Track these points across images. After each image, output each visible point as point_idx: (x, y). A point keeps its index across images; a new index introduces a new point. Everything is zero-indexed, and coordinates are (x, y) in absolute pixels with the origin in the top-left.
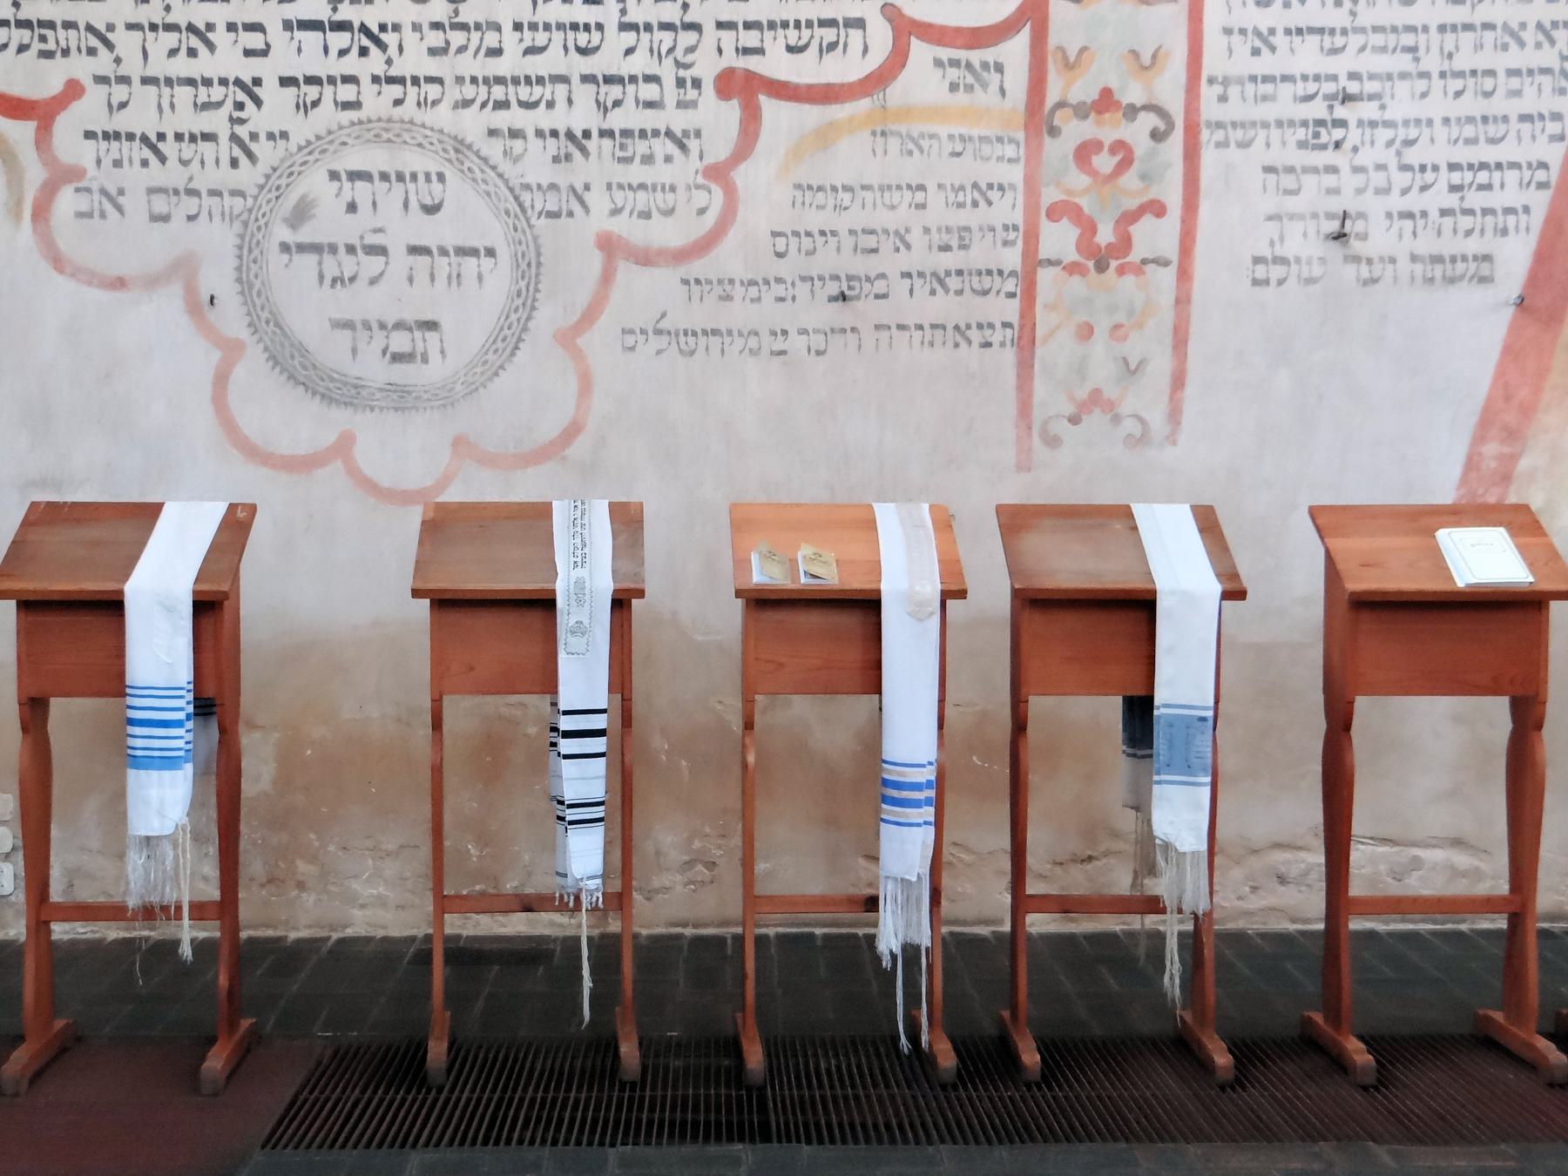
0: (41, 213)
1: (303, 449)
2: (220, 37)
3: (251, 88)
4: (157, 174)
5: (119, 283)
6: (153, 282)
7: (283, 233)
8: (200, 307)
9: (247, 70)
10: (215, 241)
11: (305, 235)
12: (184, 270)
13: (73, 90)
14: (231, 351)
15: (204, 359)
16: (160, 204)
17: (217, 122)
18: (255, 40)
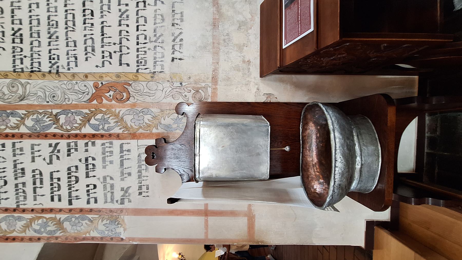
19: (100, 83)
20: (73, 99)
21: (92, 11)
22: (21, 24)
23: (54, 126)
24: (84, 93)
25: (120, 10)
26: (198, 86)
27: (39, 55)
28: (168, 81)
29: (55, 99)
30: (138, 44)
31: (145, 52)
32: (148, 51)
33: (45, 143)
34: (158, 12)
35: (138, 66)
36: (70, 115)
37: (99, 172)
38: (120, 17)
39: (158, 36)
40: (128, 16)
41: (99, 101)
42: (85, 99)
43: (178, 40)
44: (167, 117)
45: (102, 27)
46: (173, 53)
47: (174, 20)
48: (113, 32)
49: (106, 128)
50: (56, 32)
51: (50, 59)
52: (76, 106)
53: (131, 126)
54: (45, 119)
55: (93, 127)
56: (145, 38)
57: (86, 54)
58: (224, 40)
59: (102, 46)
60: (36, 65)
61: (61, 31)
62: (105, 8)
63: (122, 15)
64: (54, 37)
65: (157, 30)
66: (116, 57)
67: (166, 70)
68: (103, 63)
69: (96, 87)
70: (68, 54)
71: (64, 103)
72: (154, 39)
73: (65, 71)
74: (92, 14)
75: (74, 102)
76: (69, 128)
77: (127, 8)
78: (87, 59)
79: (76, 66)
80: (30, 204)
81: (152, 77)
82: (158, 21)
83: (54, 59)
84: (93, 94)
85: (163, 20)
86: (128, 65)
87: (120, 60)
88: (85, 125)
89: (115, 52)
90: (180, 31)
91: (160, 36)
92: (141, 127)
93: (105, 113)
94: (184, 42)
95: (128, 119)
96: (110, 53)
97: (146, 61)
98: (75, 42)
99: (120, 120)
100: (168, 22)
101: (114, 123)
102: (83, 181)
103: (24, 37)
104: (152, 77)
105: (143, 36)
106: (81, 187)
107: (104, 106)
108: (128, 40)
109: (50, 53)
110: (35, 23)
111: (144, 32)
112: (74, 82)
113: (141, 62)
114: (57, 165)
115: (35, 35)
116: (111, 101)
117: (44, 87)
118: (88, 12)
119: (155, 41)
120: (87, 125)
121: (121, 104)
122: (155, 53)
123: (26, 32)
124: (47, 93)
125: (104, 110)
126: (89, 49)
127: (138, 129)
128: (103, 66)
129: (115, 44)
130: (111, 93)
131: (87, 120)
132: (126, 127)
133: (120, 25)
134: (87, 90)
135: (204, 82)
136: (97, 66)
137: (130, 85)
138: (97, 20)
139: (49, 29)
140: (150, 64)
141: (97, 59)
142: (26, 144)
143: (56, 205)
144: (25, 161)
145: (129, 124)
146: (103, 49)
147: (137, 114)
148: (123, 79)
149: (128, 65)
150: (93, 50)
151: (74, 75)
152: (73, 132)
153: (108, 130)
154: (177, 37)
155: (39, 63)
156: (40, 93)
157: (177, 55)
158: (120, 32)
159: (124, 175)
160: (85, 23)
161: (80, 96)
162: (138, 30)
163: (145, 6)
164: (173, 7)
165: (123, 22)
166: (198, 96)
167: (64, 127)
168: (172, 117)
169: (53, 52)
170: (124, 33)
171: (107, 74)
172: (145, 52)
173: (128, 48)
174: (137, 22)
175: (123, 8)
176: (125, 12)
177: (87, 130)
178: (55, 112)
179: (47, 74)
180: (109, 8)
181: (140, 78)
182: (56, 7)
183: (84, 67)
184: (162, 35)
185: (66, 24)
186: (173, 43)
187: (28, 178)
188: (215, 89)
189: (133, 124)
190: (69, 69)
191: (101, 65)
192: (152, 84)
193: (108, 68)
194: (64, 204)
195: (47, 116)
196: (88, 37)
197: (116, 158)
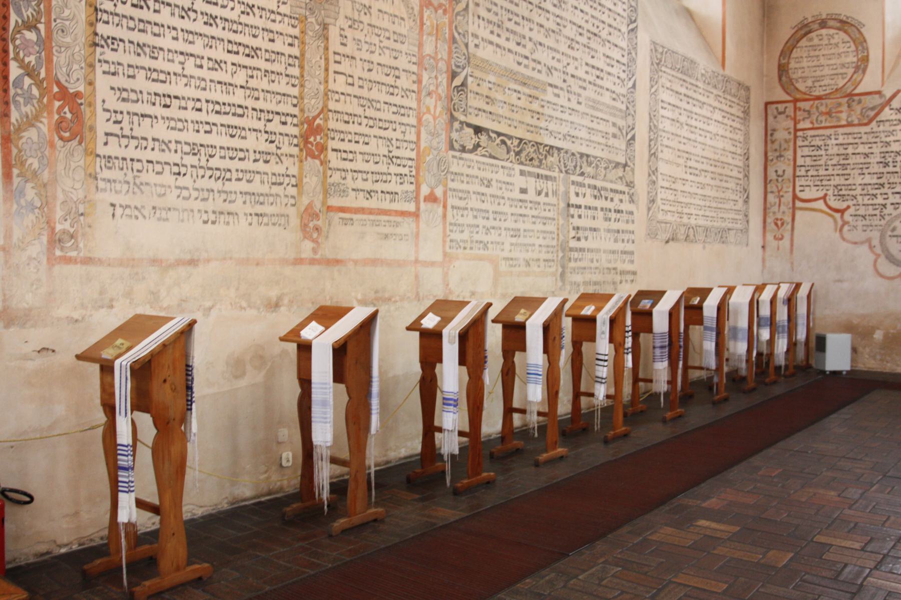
0: (841, 230)
1: (892, 275)
2: (879, 196)
3: (884, 206)
4: (864, 222)
5: (855, 243)
6: (862, 243)
7: (889, 233)
8: (871, 248)
9: (884, 202)
10: (875, 235)
11: (895, 233)
12: (869, 241)
13: (848, 207)
14: (878, 256)
15: (872, 257)
16: (865, 228)
17: (877, 212)
18: (886, 196)
19: (82, 101)
20: (60, 59)
21: (169, 107)
22: (155, 11)
23: (20, 21)
24: (68, 75)
25: (170, 142)
26: (79, 239)
27: (118, 25)
28: (85, 197)
29: (60, 32)
30: (132, 160)
31: (122, 169)
32: (122, 173)
34: (168, 190)
35: (104, 157)
36: (37, 48)
38: (163, 141)
39: (142, 187)
40: (163, 151)
41: (57, 96)
42: (60, 76)
43: (137, 213)
44: (34, 191)
45: (150, 117)
46: (121, 206)
47: (160, 209)
48: (144, 129)
49: (18, 98)
50: (145, 54)
51: (113, 38)
52: (49, 60)
53: (22, 137)
54: (30, 10)
55: (19, 79)
56: (138, 171)
57: (119, 89)
58: (137, 274)
59: (128, 113)
60: (105, 17)
61: (145, 61)
62: (173, 124)
63: (165, 143)
64: (139, 51)
65: (148, 187)
66: (115, 129)
67: (100, 196)
68: (108, 111)
69: (78, 94)
70: (119, 64)
71: (54, 44)
72: (138, 182)
73: (98, 56)
74: (166, 106)
75: (55, 59)
76: (18, 42)
77: (173, 151)
78: (112, 88)
79: (104, 72)
81: (90, 175)
82: (158, 189)
83: (113, 43)
84: (67, 88)
85: (160, 196)
86: (106, 144)
87: (111, 134)
88: (21, 67)
89: (122, 129)
90: (147, 216)
91: (141, 190)
92: (20, 151)
93: (40, 101)
94: (134, 220)
95: (31, 134)
96: (120, 122)
97: (110, 168)
98: (133, 77)
99: (30, 122)
100: (159, 202)
101: (26, 113)
103: (138, 10)
104: (90, 175)
105: (140, 168)
107: (50, 102)
108: (136, 147)
109: (121, 40)
110: (156, 29)
111: (145, 170)
112: (83, 65)
113: (109, 162)
115: (141, 26)
116: (59, 112)
117: (74, 21)
118: (168, 101)
119: (135, 184)
120: (21, 71)
121: (53, 127)
122: (120, 182)
124: (67, 23)
125: (45, 100)
126: (125, 95)
127: (17, 147)
128: (105, 110)
129: (132, 129)
130: (69, 116)
131: (30, 72)
132: (19, 130)
133: (154, 140)
134: (72, 81)
135: (85, 246)
136: (104, 101)
137: (80, 143)
138: (158, 111)
139: (149, 46)
140: (107, 174)
141: (113, 103)
145: (25, 134)
146: (125, 113)
147: (40, 149)
148: (88, 135)
149: (106, 144)
150: (124, 100)
151: (92, 66)
152: (11, 48)
153: (15, 102)
154: (140, 212)
155: (107, 23)
156: (67, 13)
157: (119, 211)
158: (146, 139)
160: (156, 94)
161: (64, 70)
162: (148, 162)
163: (175, 174)
164: (174, 209)
165: (157, 143)
166: (66, 237)
167: (18, 36)
168: (36, 199)
169: (121, 44)
170: (144, 143)
171: (94, 113)
172: (122, 169)
173: (126, 146)
174: (158, 162)
175: (173, 146)
176: (168, 148)
178: (41, 27)
179: (93, 28)
180: (172, 128)
181: (90, 158)
182: (173, 61)
183: (103, 83)
184: (142, 192)
185: (155, 70)
186: (133, 207)
188: (76, 262)
189: (24, 140)
190: (100, 61)
191: (106, 106)
192: (80, 175)
193: (101, 116)
195: (34, 13)
196: (140, 96)
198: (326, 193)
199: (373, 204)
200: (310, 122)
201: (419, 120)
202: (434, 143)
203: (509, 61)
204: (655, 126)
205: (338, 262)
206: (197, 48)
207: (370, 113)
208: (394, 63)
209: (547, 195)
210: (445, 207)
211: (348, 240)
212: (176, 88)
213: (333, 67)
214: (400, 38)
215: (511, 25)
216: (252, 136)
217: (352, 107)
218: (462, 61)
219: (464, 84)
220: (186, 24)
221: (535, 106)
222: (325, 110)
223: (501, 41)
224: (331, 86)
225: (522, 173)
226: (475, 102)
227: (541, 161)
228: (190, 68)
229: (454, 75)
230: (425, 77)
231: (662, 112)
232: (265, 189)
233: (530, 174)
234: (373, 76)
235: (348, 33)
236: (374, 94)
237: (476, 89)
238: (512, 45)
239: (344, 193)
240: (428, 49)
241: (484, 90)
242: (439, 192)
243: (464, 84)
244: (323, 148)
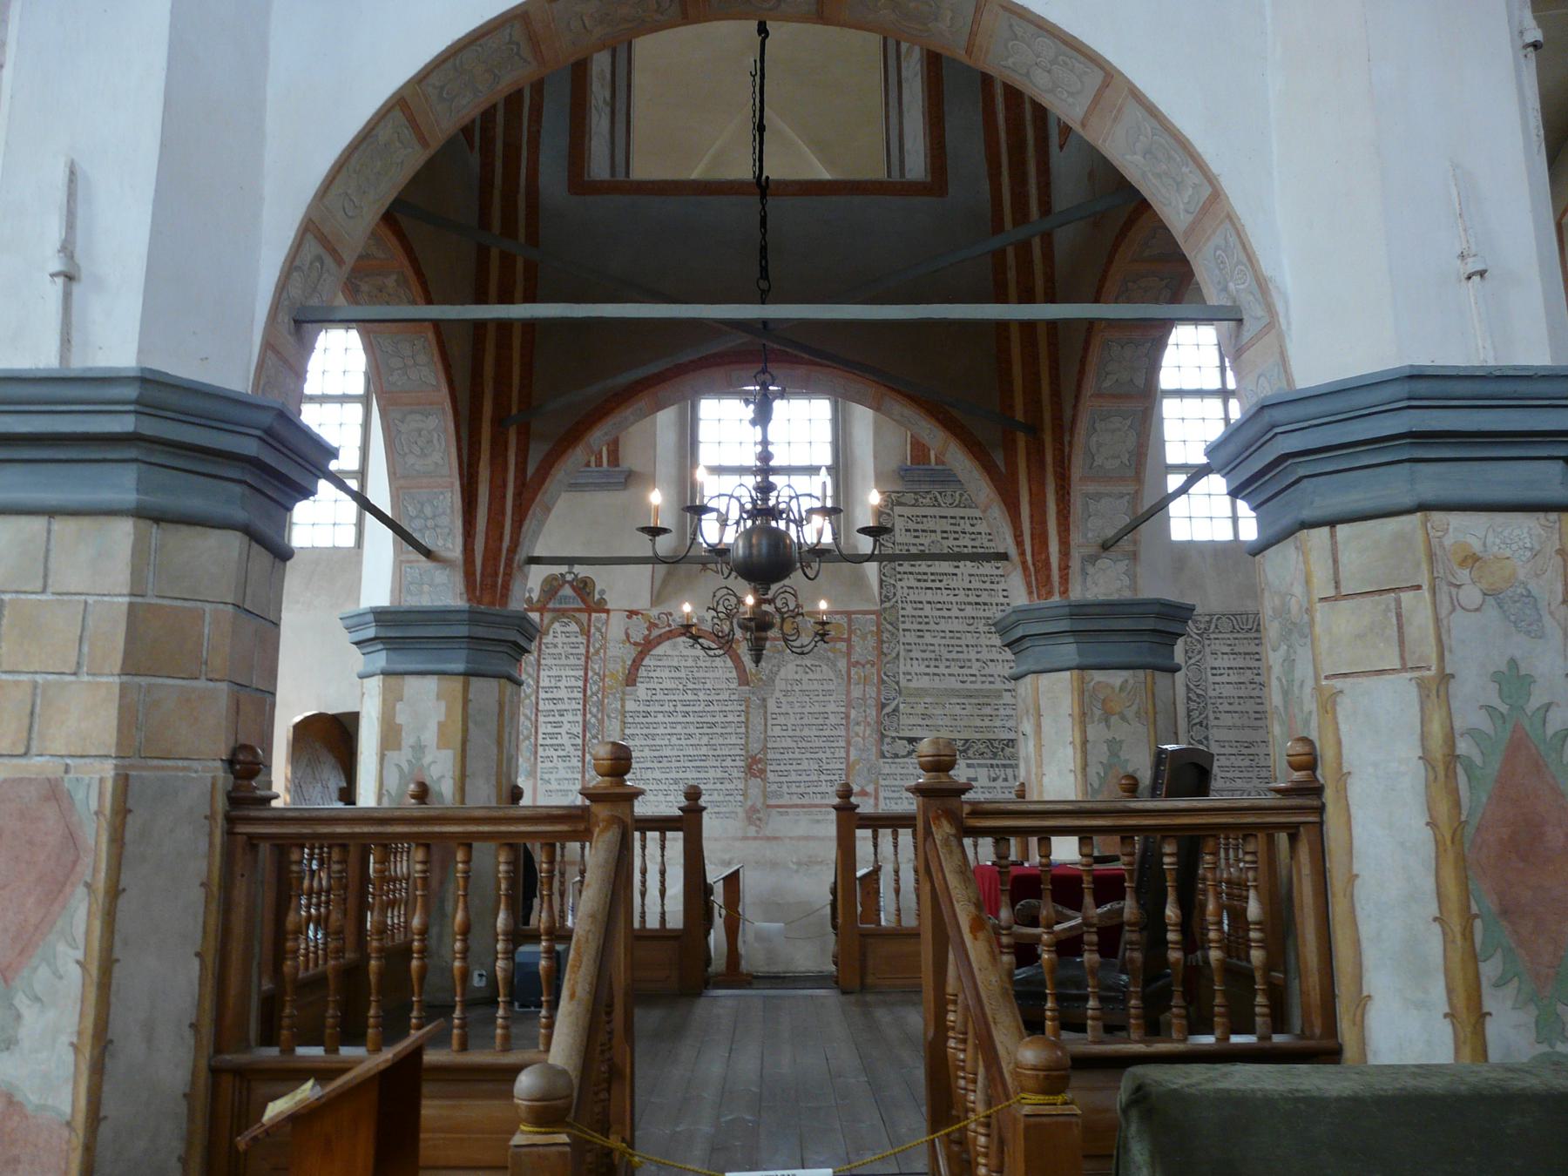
33: (580, 730)
37: (561, 765)
80: (541, 719)
102: (555, 754)
106: (551, 752)
114: (566, 737)
123: (649, 720)
138: (656, 765)
142: (580, 718)
143: (540, 736)
144: (569, 717)
159: (559, 780)
177: (588, 757)
187: (558, 718)
194: (540, 741)
197: (570, 776)
198: (765, 795)
199: (805, 801)
200: (753, 758)
201: (848, 743)
202: (864, 756)
203: (953, 683)
204: (1198, 696)
205: (776, 838)
206: (679, 729)
207: (804, 744)
208: (822, 710)
209: (1006, 780)
210: (876, 798)
211: (779, 824)
212: (667, 752)
213: (770, 722)
214: (829, 692)
215: (954, 655)
216: (712, 771)
217: (789, 743)
218: (894, 694)
219: (896, 710)
220: (672, 719)
221: (988, 710)
222: (765, 749)
223: (942, 670)
224: (770, 733)
225: (969, 766)
226: (904, 720)
227: (995, 754)
228: (674, 740)
229: (884, 706)
230: (853, 713)
231: (1217, 679)
232: (721, 798)
233: (980, 765)
234: (805, 721)
235: (783, 700)
236: (806, 732)
237: (910, 711)
238: (956, 671)
239: (781, 796)
240: (856, 692)
241: (920, 709)
242: (870, 789)
243: (896, 710)
244: (763, 771)
